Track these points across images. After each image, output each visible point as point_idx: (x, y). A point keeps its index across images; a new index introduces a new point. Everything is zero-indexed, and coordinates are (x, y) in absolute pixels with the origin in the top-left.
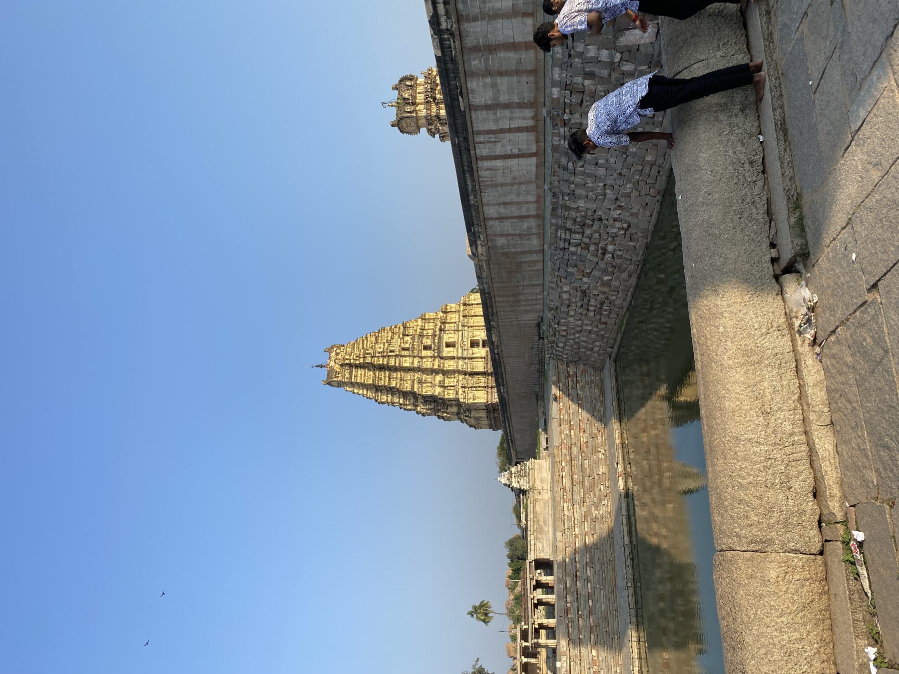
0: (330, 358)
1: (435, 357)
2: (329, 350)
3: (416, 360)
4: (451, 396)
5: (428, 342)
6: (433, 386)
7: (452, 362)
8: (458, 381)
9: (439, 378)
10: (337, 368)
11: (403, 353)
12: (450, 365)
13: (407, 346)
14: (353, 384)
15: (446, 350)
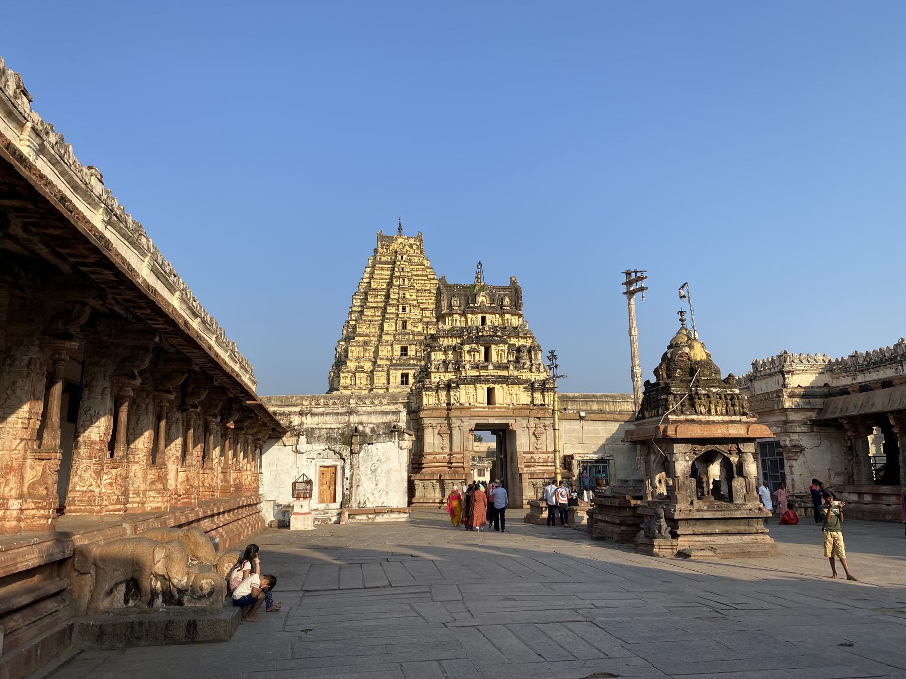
0: (409, 238)
1: (391, 360)
2: (419, 238)
3: (389, 338)
4: (342, 381)
5: (411, 352)
6: (358, 359)
7: (384, 380)
8: (360, 388)
9: (368, 366)
10: (394, 246)
11: (400, 323)
12: (380, 379)
13: (409, 327)
14: (373, 266)
15: (399, 374)
